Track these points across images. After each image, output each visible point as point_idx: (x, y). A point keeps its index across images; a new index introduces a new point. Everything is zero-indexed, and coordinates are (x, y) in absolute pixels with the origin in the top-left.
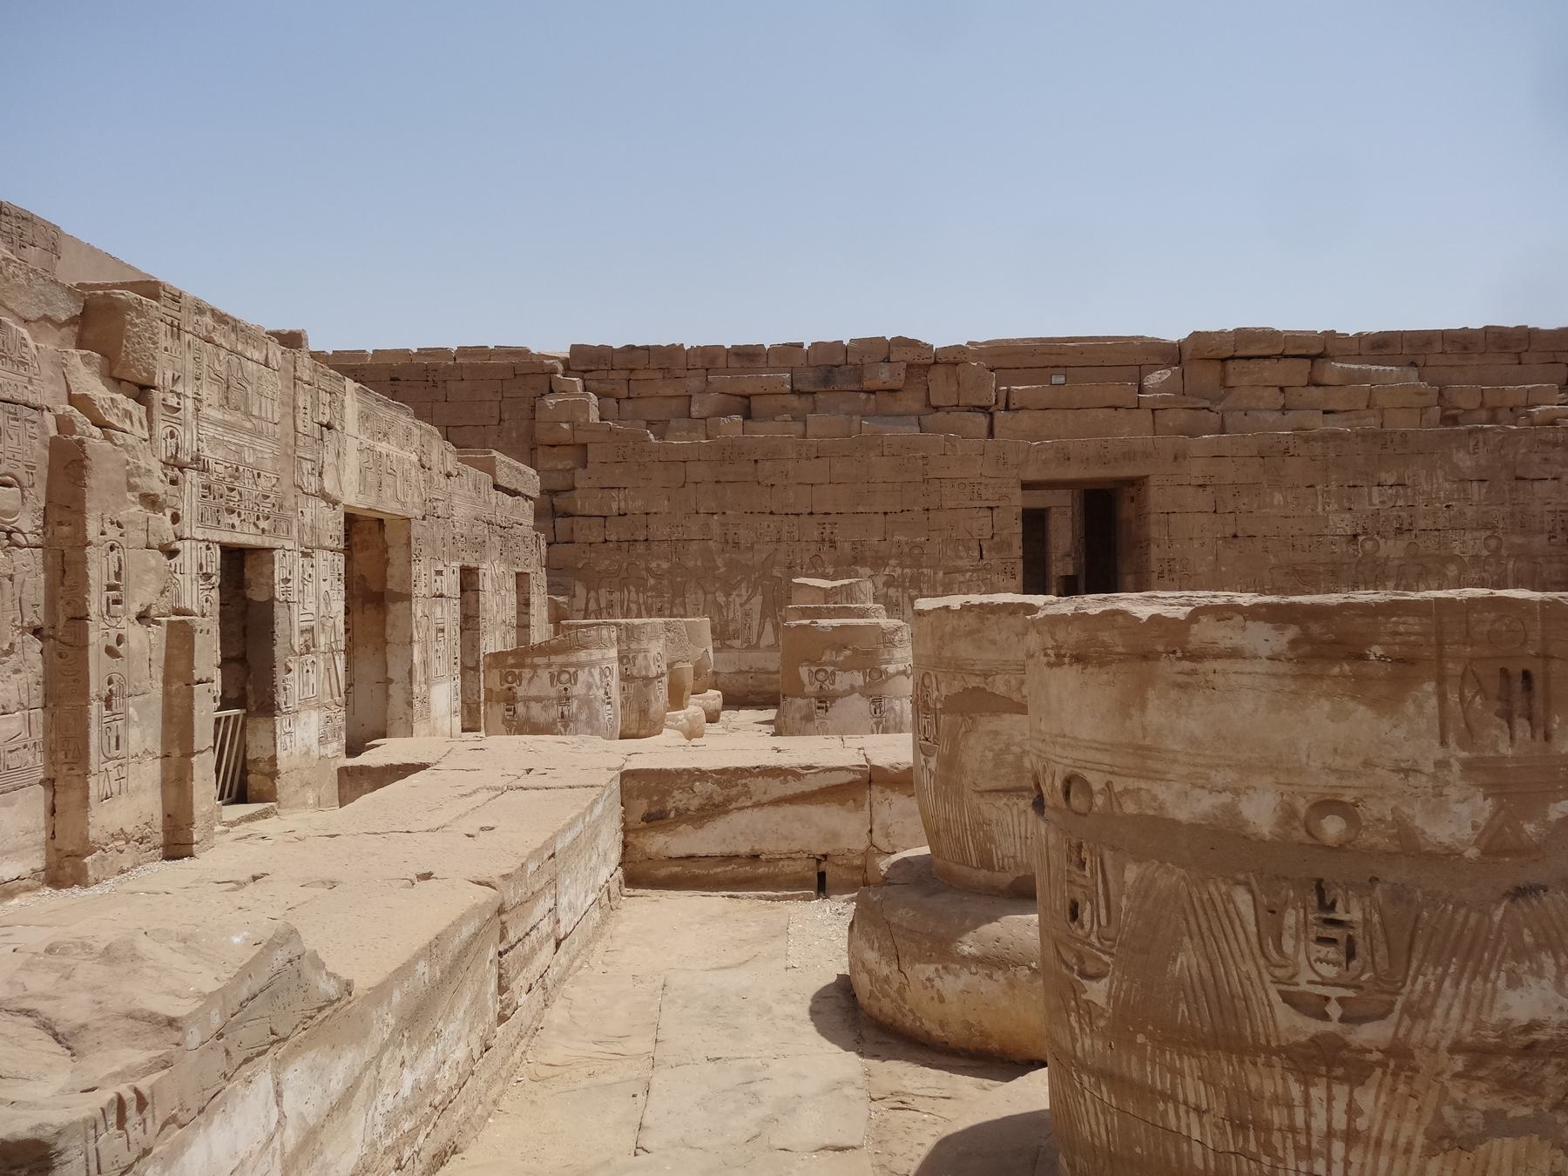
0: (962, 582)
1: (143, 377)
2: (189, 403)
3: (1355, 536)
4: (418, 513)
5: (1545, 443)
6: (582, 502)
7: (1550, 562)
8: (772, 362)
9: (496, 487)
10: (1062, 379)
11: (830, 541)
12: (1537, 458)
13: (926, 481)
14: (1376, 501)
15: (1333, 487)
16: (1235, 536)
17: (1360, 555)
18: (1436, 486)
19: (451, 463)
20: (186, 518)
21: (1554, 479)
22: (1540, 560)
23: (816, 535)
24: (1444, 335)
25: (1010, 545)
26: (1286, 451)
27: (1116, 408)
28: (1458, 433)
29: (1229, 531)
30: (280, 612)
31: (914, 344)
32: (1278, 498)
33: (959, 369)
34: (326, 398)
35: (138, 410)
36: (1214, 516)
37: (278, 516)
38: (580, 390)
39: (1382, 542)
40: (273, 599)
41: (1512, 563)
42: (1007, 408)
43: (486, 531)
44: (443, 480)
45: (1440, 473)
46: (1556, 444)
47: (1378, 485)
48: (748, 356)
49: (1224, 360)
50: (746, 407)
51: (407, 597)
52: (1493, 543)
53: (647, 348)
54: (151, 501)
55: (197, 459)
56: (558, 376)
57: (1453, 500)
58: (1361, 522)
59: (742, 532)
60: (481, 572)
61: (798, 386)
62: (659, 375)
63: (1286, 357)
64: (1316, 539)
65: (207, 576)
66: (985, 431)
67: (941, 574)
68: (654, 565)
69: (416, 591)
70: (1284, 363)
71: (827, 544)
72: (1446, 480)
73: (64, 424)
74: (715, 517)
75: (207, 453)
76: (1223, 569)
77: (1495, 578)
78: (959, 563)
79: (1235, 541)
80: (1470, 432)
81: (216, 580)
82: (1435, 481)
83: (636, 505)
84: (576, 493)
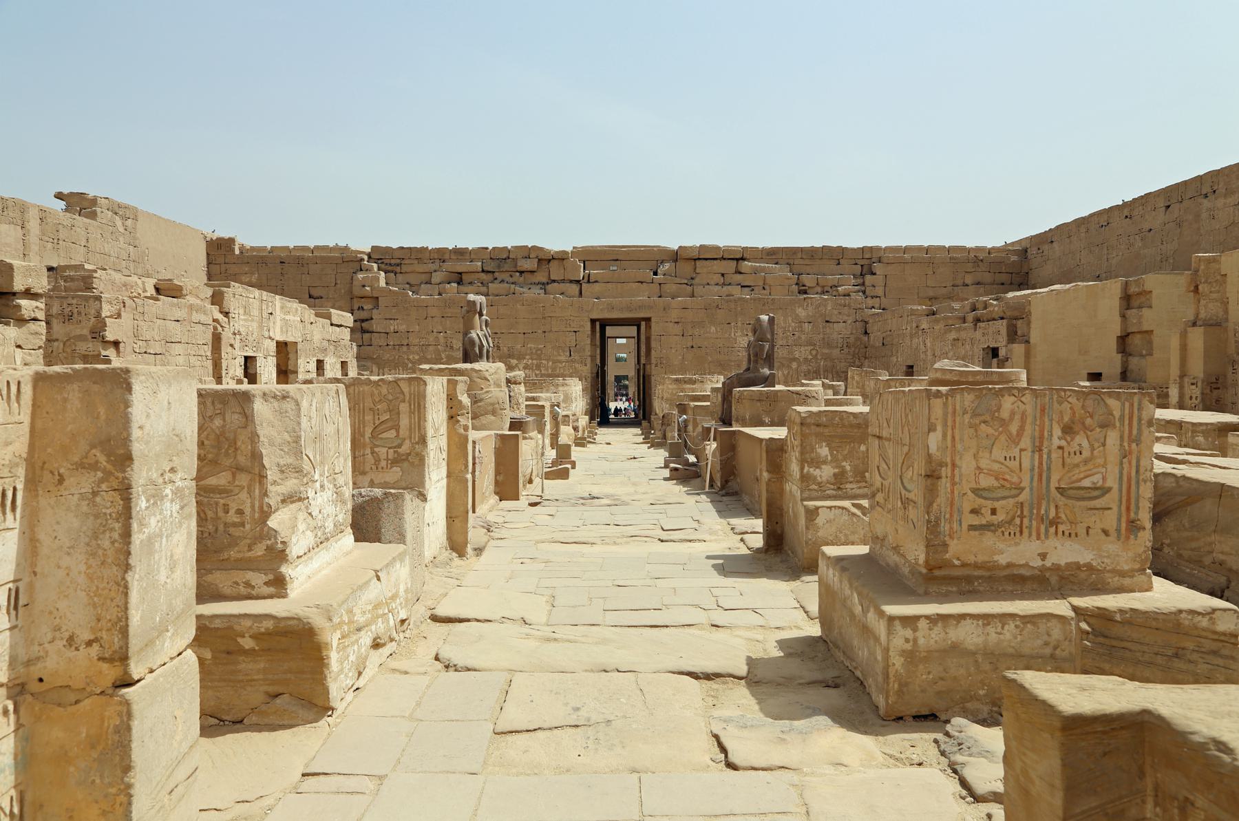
1: (227, 311)
2: (237, 315)
4: (300, 340)
6: (375, 325)
9: (332, 325)
10: (615, 268)
12: (836, 312)
13: (543, 318)
15: (739, 324)
16: (692, 347)
19: (313, 318)
24: (802, 249)
25: (584, 350)
26: (717, 306)
27: (642, 282)
28: (800, 300)
29: (689, 344)
30: (258, 376)
31: (541, 249)
32: (713, 329)
33: (565, 261)
34: (270, 304)
35: (226, 319)
37: (257, 347)
38: (376, 269)
40: (256, 373)
42: (589, 282)
44: (309, 325)
45: (790, 319)
46: (845, 306)
48: (460, 253)
49: (695, 260)
50: (459, 278)
51: (296, 372)
52: (814, 352)
53: (410, 248)
54: (231, 345)
56: (366, 262)
59: (454, 341)
61: (485, 269)
62: (416, 262)
63: (725, 259)
66: (577, 293)
67: (551, 363)
68: (411, 357)
69: (299, 370)
70: (723, 262)
73: (215, 328)
75: (241, 330)
78: (559, 358)
80: (805, 299)
83: (403, 328)
84: (373, 321)
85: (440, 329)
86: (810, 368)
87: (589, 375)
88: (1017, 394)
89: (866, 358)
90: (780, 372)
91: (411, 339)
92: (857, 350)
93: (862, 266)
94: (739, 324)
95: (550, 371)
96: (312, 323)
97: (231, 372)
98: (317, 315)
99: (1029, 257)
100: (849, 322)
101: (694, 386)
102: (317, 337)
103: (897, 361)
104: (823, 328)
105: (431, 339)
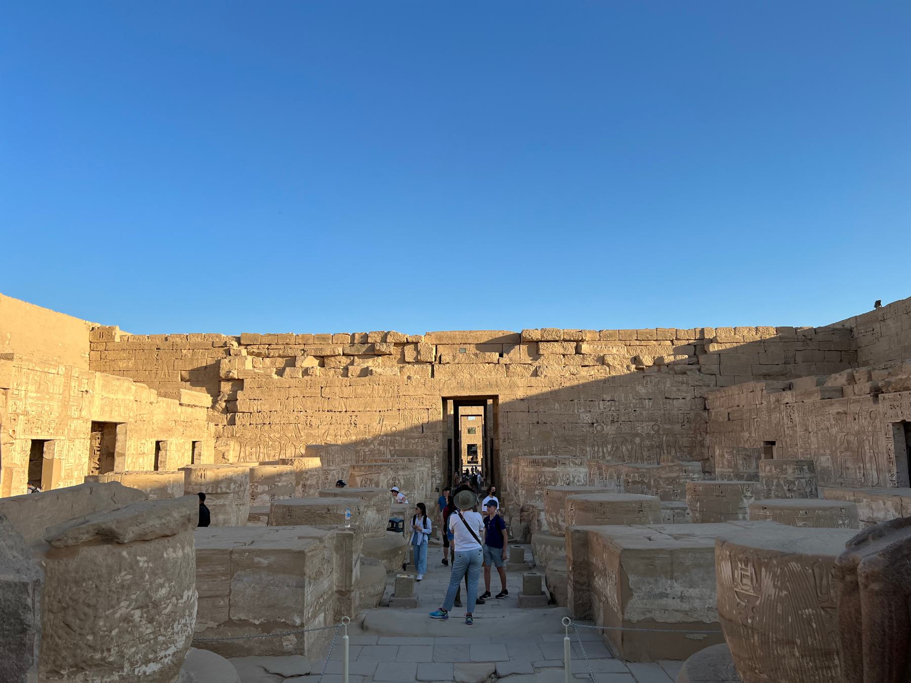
0: (414, 443)
5: (678, 382)
7: (683, 437)
8: (334, 341)
12: (674, 389)
14: (602, 407)
15: (582, 401)
17: (595, 433)
21: (683, 399)
22: (678, 436)
23: (348, 421)
29: (535, 421)
39: (605, 427)
41: (665, 437)
43: (174, 424)
45: (631, 395)
46: (683, 383)
47: (603, 400)
52: (656, 428)
57: (637, 408)
58: (595, 417)
59: (313, 419)
64: (575, 425)
67: (404, 439)
72: (634, 399)
76: (533, 438)
77: (657, 444)
78: (413, 434)
79: (537, 425)
82: (628, 399)
83: (266, 408)
85: (300, 407)
86: (653, 443)
87: (441, 450)
89: (707, 433)
90: (624, 448)
92: (698, 426)
93: (695, 346)
94: (582, 401)
98: (159, 395)
99: (856, 336)
100: (688, 398)
101: (555, 469)
103: (750, 436)
104: (663, 404)
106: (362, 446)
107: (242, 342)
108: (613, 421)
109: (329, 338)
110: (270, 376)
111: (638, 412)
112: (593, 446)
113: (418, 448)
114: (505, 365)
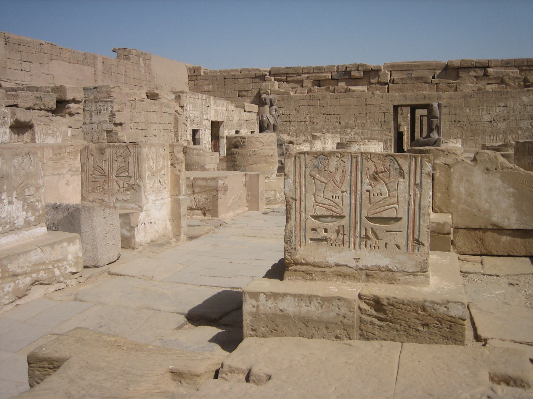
0: (375, 134)
1: (183, 105)
3: (491, 122)
8: (326, 70)
9: (245, 111)
11: (339, 122)
13: (366, 105)
14: (498, 111)
18: (516, 107)
19: (233, 108)
20: (188, 126)
23: (335, 120)
29: (453, 119)
36: (448, 115)
37: (201, 124)
39: (499, 123)
42: (393, 83)
44: (231, 112)
47: (499, 106)
49: (458, 68)
55: (189, 116)
59: (315, 119)
60: (241, 132)
65: (191, 135)
67: (369, 131)
68: (291, 128)
71: (338, 123)
74: (308, 115)
81: (192, 135)
83: (287, 112)
85: (307, 112)
88: (339, 156)
91: (291, 118)
94: (485, 107)
95: (369, 136)
96: (233, 111)
97: (184, 138)
98: (236, 106)
102: (236, 118)
105: (303, 119)
106: (344, 135)
107: (271, 73)
108: (504, 120)
109: (322, 69)
110: (289, 93)
111: (522, 114)
112: (490, 136)
113: (378, 137)
114: (436, 84)
